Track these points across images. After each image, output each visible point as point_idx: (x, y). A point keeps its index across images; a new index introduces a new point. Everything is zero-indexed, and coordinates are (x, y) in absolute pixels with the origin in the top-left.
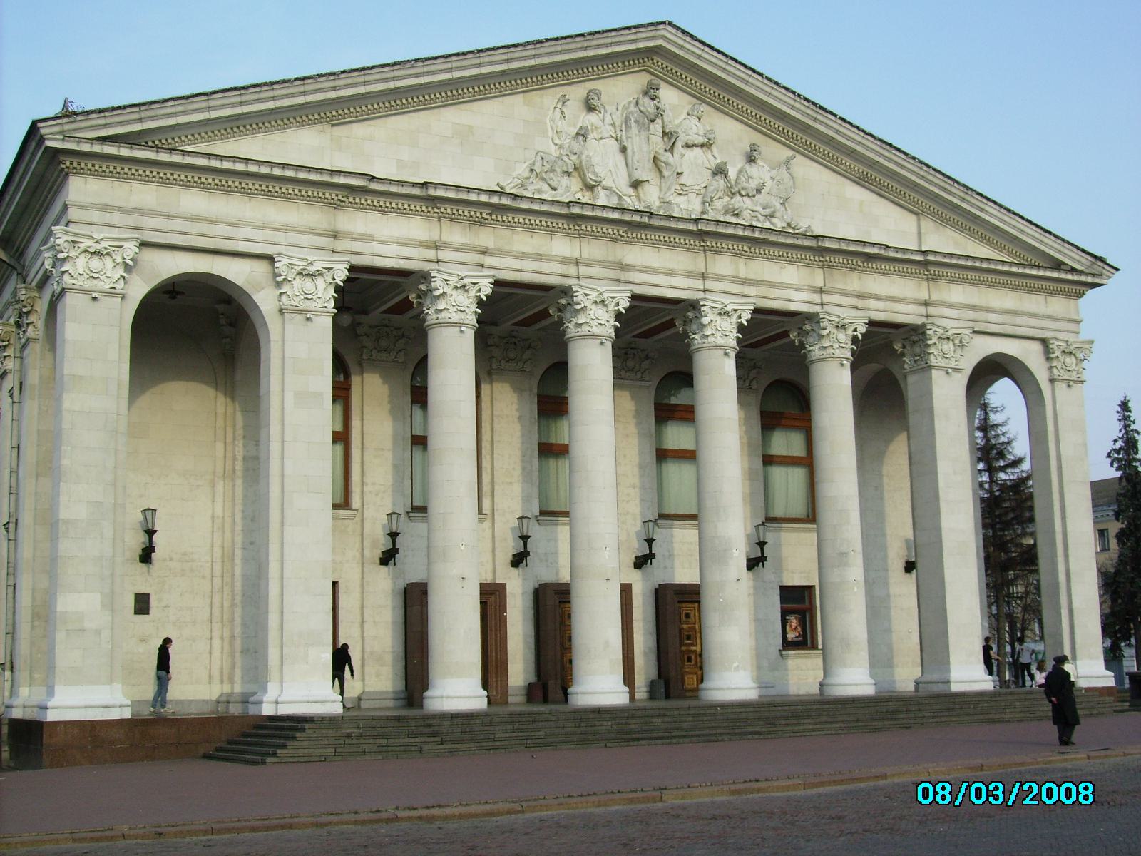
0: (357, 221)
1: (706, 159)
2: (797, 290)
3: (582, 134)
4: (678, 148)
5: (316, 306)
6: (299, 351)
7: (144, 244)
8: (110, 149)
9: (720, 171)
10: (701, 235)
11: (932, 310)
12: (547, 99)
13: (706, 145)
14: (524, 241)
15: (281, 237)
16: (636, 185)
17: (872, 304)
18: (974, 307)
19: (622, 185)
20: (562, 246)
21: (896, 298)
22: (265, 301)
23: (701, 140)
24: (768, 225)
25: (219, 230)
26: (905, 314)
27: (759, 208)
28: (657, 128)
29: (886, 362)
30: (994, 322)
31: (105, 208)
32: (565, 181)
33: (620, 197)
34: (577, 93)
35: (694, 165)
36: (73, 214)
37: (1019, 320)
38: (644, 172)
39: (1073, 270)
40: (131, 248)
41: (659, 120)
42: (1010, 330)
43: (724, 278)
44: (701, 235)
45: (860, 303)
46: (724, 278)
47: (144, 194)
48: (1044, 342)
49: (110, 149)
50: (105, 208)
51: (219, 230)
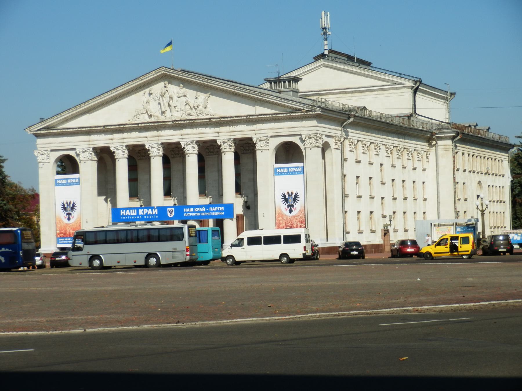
0: (94, 137)
1: (180, 101)
3: (147, 102)
4: (175, 98)
5: (87, 158)
6: (89, 168)
7: (52, 150)
8: (39, 132)
10: (179, 125)
12: (141, 93)
15: (79, 144)
16: (163, 113)
18: (272, 129)
19: (158, 114)
23: (182, 95)
24: (201, 117)
25: (66, 144)
26: (247, 135)
27: (199, 112)
28: (167, 95)
29: (245, 149)
31: (43, 144)
32: (142, 116)
33: (157, 117)
34: (147, 90)
35: (179, 103)
36: (38, 146)
38: (165, 108)
39: (307, 111)
40: (49, 152)
41: (167, 93)
43: (188, 134)
44: (179, 125)
45: (232, 134)
46: (188, 134)
48: (300, 135)
49: (39, 132)
50: (43, 144)
51: (66, 144)
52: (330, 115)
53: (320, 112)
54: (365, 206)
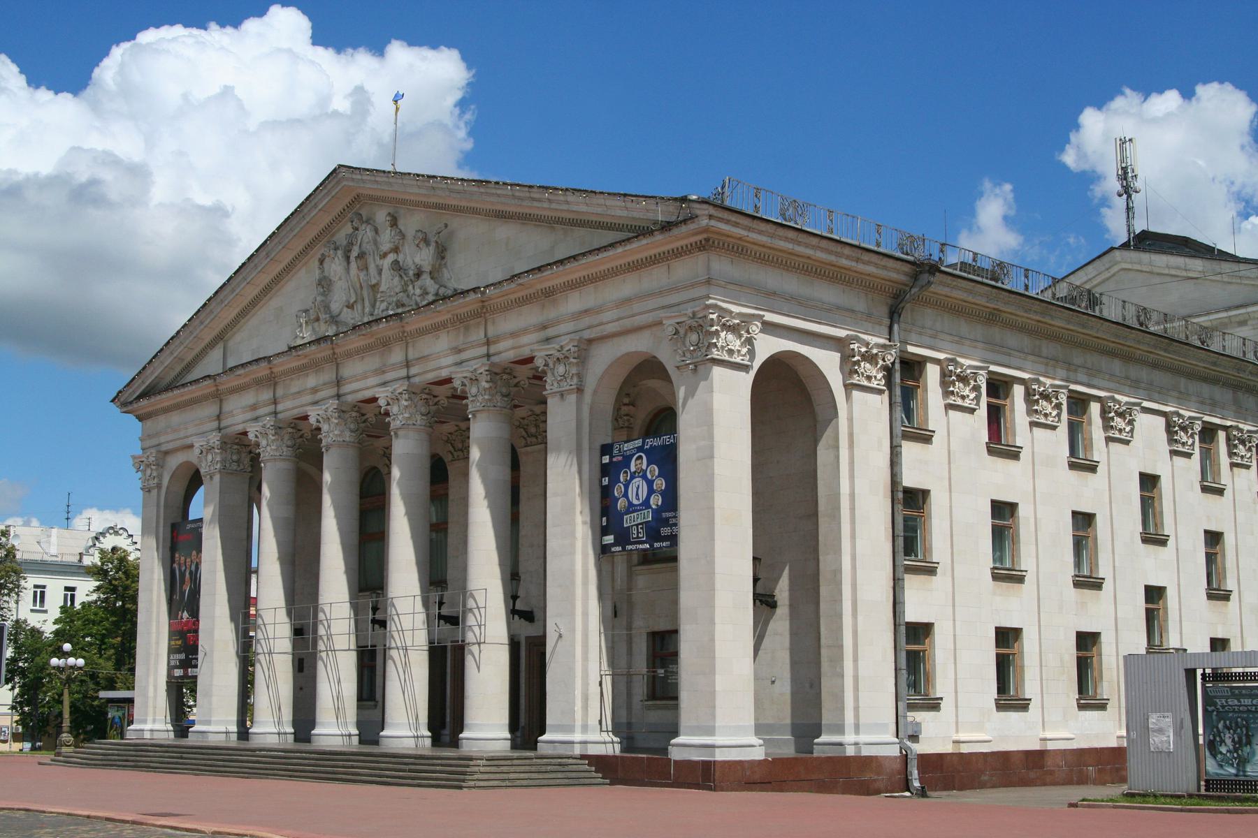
2: (445, 356)
9: (396, 266)
11: (550, 332)
13: (396, 250)
14: (296, 386)
17: (502, 346)
18: (586, 312)
20: (311, 381)
21: (517, 333)
22: (202, 471)
26: (528, 344)
28: (354, 254)
30: (610, 321)
37: (637, 307)
42: (628, 323)
43: (394, 367)
47: (161, 422)
52: (800, 249)
53: (704, 222)
54: (1049, 615)
